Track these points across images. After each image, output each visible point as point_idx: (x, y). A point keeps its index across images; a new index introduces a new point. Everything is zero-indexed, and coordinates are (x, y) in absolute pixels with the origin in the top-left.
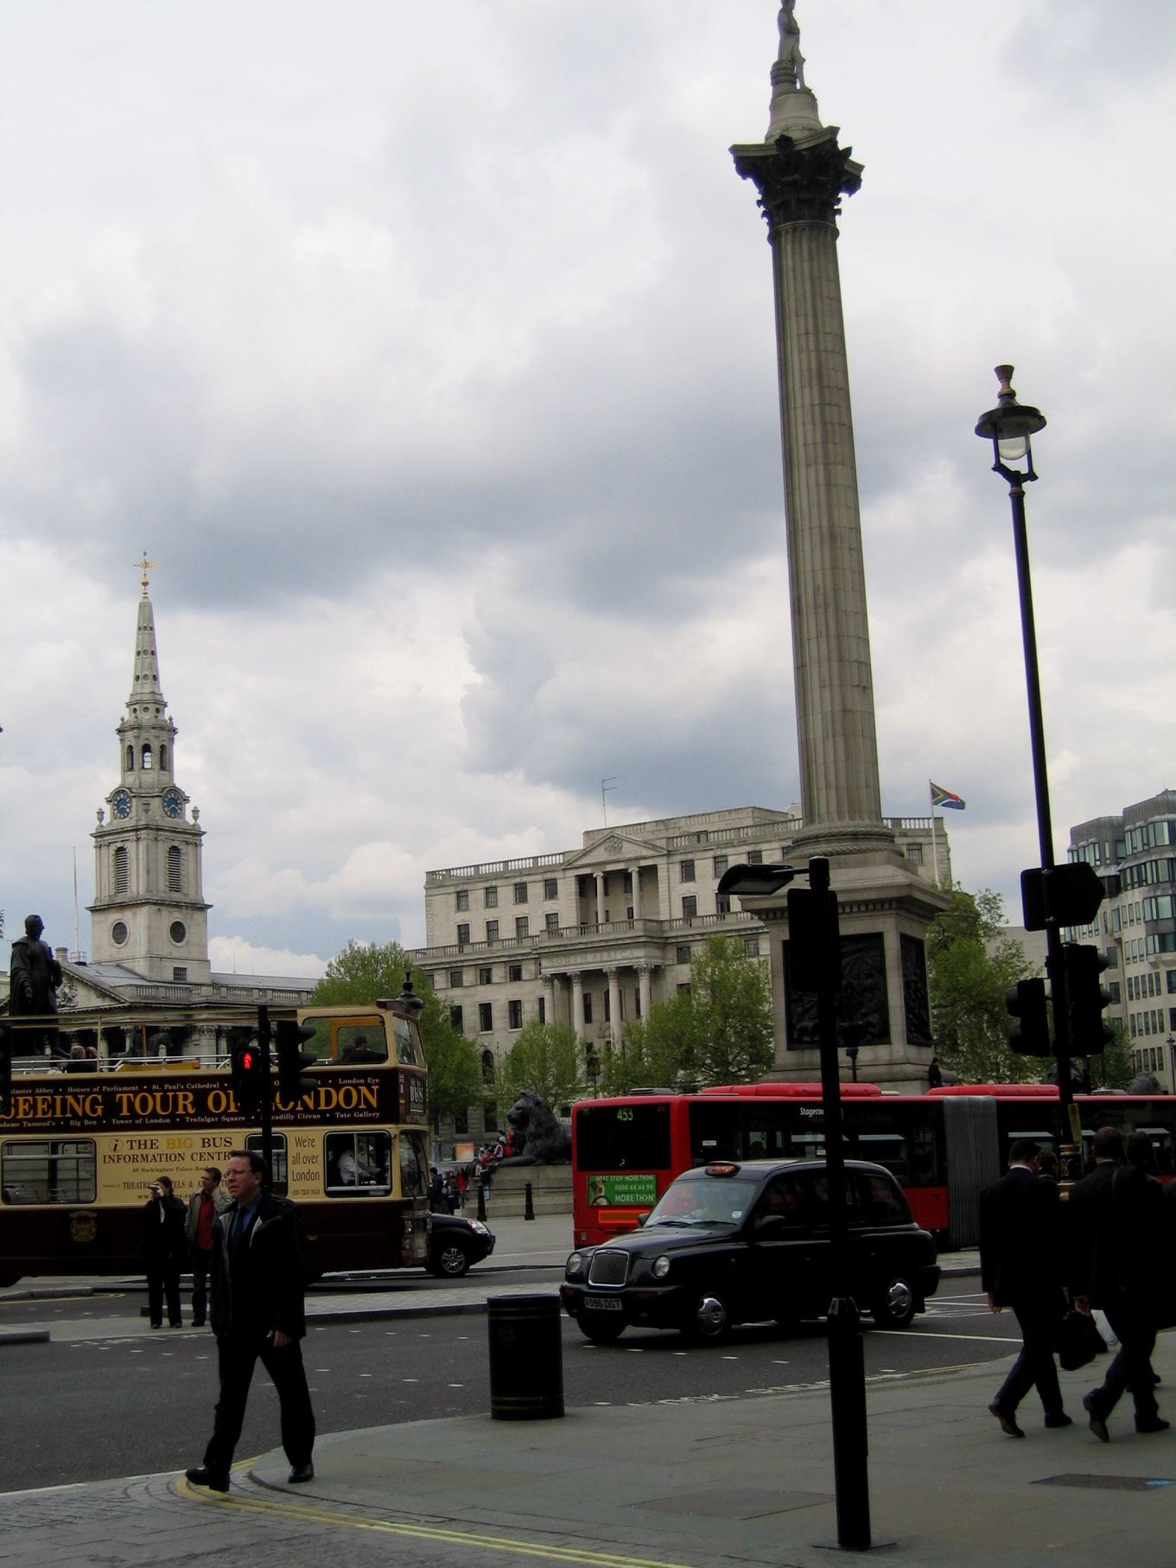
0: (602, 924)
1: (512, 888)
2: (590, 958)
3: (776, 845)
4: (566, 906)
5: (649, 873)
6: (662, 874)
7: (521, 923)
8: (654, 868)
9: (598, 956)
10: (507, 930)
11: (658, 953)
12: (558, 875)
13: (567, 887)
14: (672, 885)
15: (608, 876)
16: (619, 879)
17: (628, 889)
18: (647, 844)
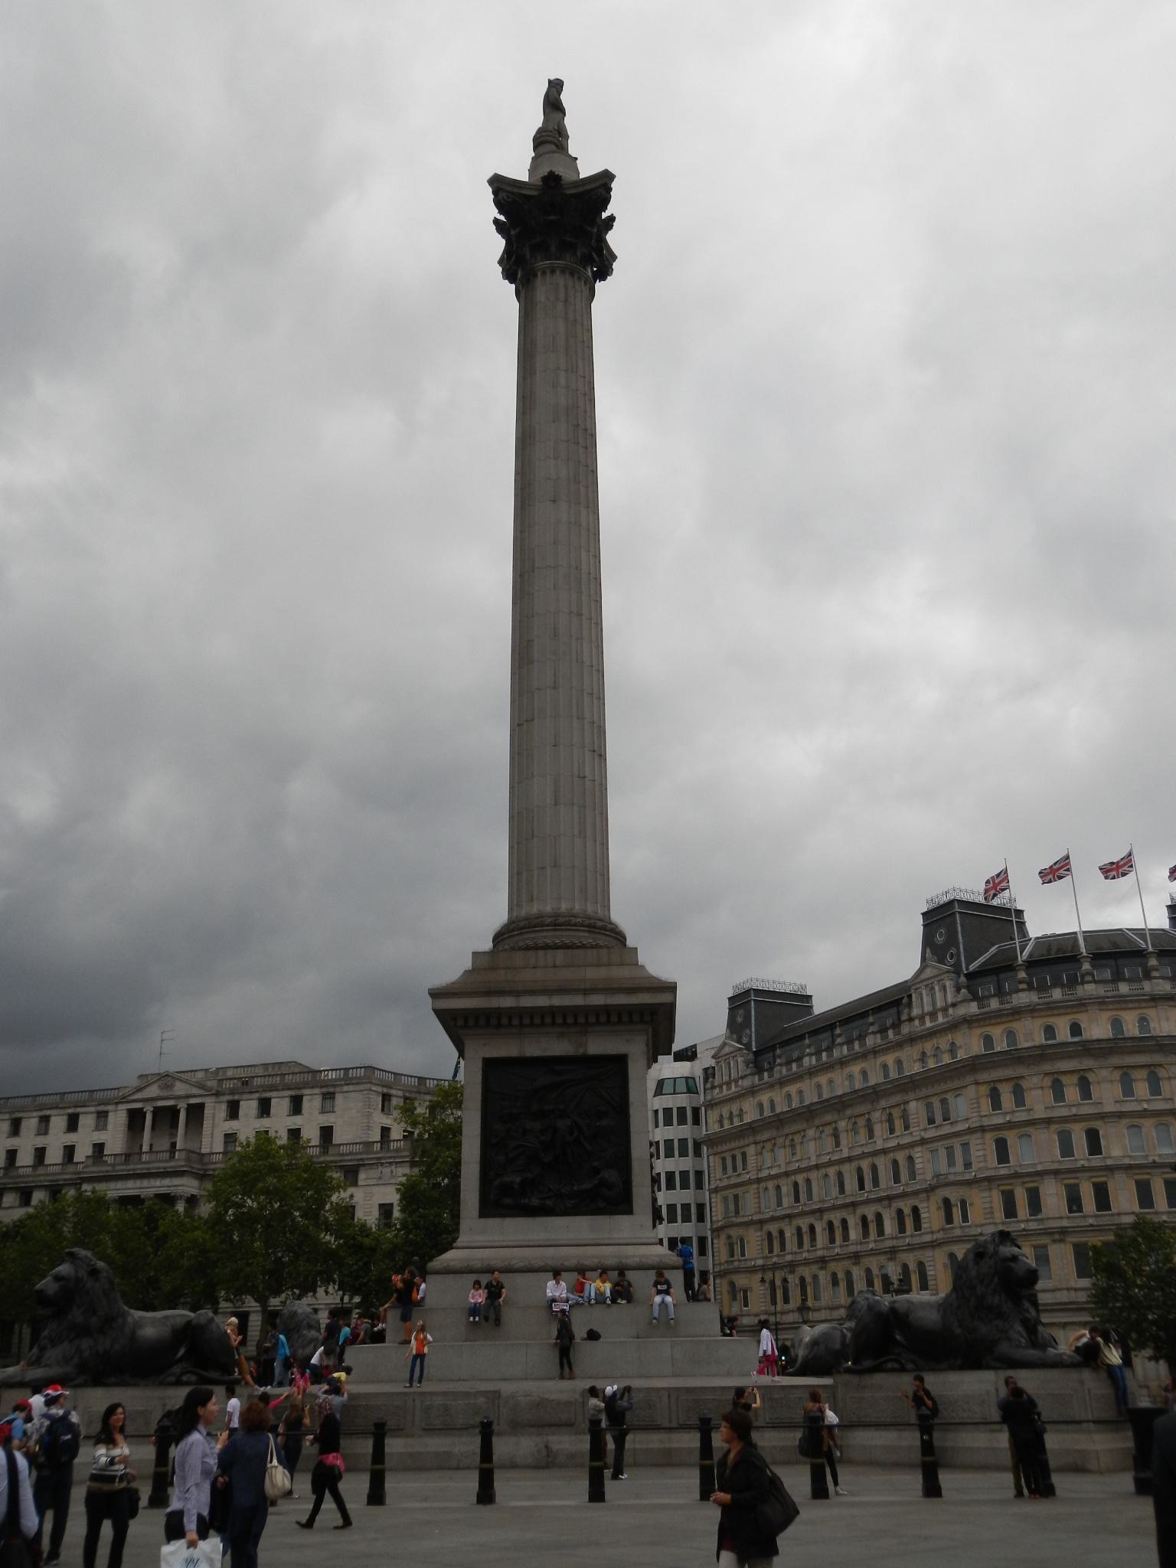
0: (146, 1153)
1: (65, 1118)
2: (130, 1184)
3: (317, 1091)
4: (114, 1138)
5: (196, 1112)
6: (207, 1111)
7: (69, 1151)
8: (201, 1106)
9: (138, 1183)
10: (54, 1156)
11: (195, 1183)
12: (110, 1108)
13: (118, 1119)
14: (216, 1121)
15: (157, 1111)
16: (167, 1117)
17: (174, 1125)
18: (200, 1085)
